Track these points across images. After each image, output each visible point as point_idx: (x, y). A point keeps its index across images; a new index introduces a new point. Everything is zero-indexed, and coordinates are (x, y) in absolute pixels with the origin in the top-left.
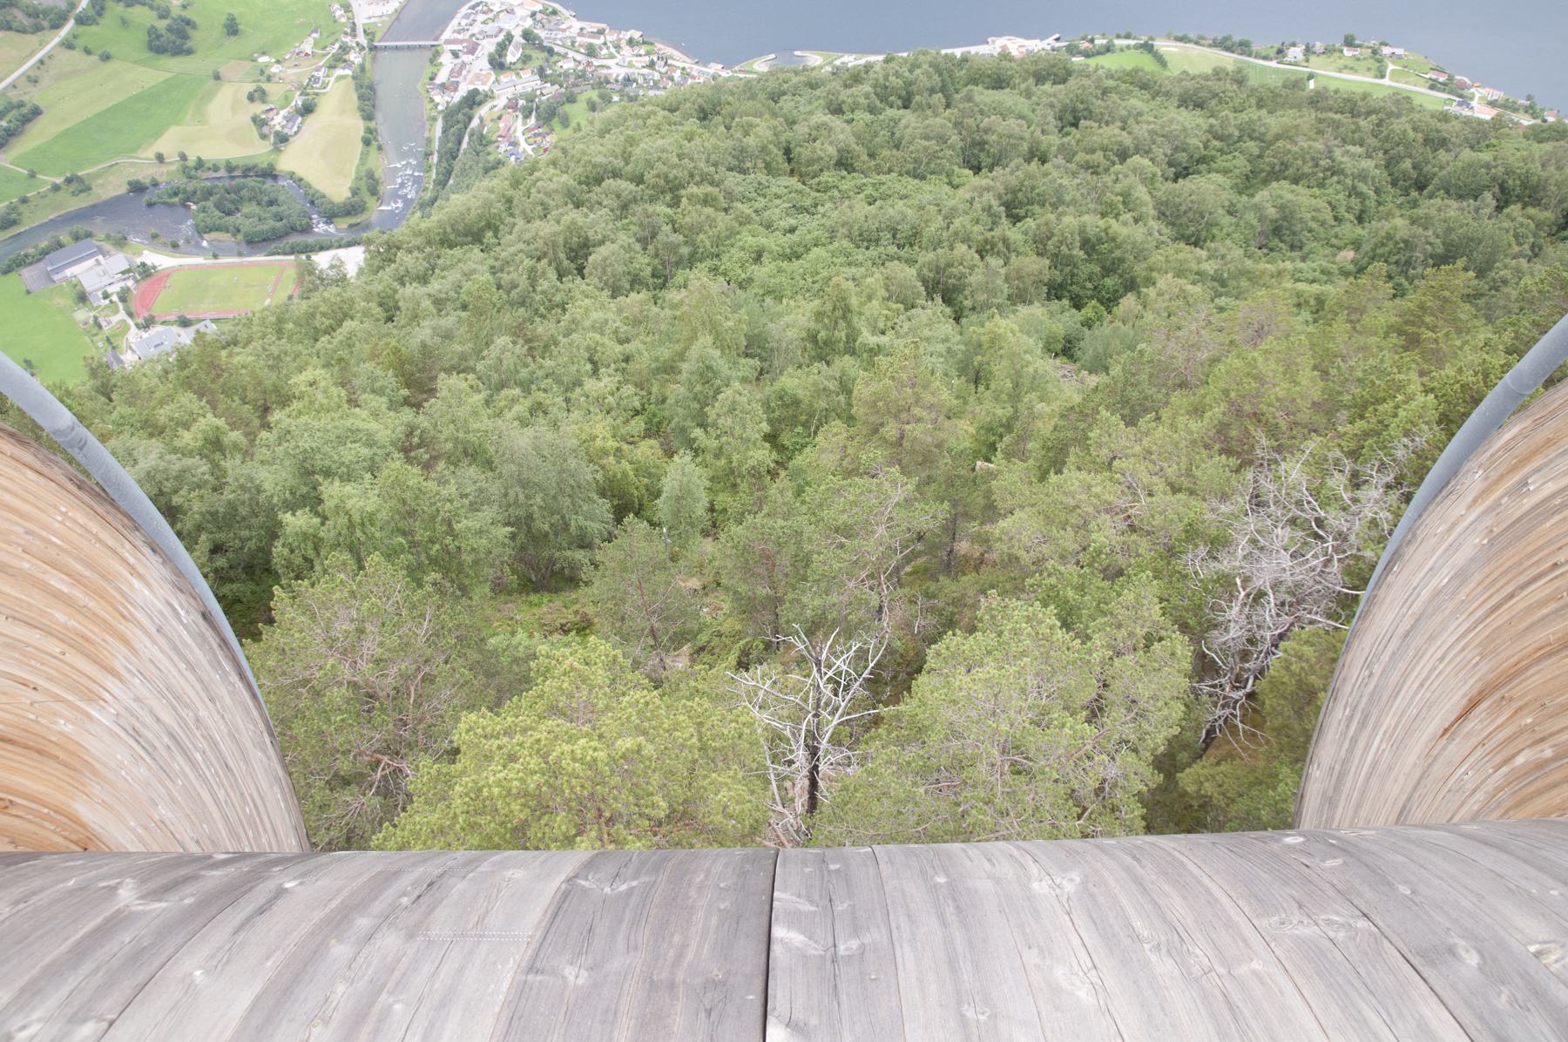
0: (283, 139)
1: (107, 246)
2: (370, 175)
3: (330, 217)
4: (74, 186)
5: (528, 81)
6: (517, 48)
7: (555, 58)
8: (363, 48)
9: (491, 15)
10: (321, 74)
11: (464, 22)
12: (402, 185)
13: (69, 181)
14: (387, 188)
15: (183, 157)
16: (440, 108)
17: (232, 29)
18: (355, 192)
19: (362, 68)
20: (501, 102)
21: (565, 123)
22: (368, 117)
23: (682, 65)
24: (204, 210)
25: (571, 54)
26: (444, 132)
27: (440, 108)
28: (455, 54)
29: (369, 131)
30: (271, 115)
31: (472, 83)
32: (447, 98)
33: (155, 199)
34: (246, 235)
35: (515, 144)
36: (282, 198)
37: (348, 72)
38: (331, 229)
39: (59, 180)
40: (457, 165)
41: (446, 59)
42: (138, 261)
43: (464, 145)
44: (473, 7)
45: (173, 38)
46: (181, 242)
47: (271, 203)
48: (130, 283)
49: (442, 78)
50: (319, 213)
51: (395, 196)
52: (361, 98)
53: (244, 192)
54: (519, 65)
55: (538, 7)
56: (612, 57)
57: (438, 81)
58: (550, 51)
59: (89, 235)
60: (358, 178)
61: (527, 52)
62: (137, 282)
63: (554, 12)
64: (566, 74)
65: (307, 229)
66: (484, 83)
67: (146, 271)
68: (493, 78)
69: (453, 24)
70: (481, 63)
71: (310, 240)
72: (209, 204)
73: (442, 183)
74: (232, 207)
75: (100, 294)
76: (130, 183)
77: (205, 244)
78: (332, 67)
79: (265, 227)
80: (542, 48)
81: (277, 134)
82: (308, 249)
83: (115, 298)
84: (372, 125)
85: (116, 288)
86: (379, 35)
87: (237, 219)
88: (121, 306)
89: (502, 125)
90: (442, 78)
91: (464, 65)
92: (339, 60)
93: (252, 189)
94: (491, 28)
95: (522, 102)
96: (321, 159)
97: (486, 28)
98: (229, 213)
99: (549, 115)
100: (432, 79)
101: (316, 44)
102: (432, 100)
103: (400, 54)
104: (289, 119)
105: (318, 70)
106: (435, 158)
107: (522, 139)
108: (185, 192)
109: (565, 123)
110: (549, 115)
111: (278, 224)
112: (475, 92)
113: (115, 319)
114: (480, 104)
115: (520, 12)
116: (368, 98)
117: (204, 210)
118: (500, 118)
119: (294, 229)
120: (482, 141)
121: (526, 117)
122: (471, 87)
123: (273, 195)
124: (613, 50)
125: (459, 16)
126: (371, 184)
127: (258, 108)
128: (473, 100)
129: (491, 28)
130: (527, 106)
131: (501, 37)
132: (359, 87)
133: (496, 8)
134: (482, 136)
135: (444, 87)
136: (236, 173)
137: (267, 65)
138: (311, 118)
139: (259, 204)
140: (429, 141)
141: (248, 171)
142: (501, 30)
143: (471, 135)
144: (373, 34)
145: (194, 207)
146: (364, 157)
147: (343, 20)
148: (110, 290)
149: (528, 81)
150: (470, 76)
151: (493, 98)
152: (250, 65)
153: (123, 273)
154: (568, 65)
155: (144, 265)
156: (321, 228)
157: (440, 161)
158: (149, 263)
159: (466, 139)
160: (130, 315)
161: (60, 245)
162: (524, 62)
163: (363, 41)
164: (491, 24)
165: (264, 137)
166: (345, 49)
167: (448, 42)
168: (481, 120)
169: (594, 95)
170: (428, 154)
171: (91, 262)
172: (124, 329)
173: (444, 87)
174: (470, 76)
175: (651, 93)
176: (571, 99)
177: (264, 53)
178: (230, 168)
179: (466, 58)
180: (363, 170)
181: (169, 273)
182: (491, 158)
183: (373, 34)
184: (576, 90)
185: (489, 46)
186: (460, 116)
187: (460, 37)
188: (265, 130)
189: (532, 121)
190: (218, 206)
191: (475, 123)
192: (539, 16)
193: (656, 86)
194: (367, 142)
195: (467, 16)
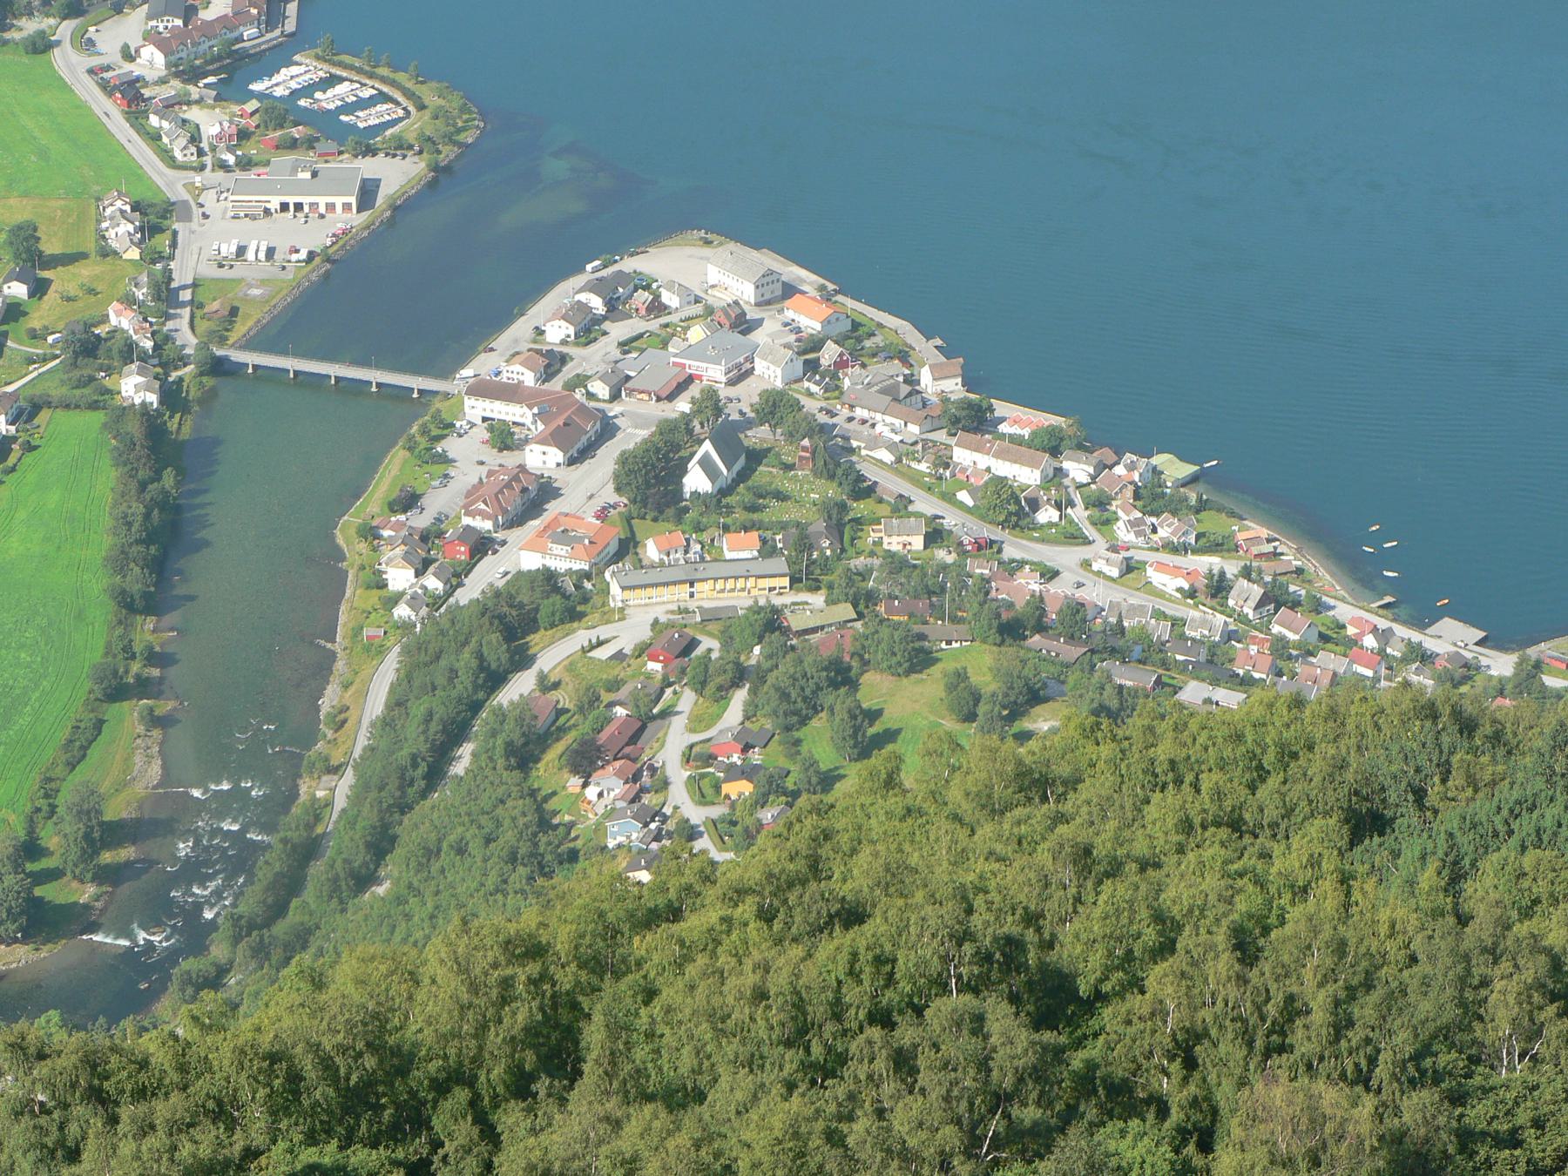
25: (925, 505)
56: (1074, 537)
69: (520, 329)
95: (709, 644)
107: (678, 775)
122: (531, 561)
124: (1079, 513)
175: (1193, 692)
193: (1215, 663)
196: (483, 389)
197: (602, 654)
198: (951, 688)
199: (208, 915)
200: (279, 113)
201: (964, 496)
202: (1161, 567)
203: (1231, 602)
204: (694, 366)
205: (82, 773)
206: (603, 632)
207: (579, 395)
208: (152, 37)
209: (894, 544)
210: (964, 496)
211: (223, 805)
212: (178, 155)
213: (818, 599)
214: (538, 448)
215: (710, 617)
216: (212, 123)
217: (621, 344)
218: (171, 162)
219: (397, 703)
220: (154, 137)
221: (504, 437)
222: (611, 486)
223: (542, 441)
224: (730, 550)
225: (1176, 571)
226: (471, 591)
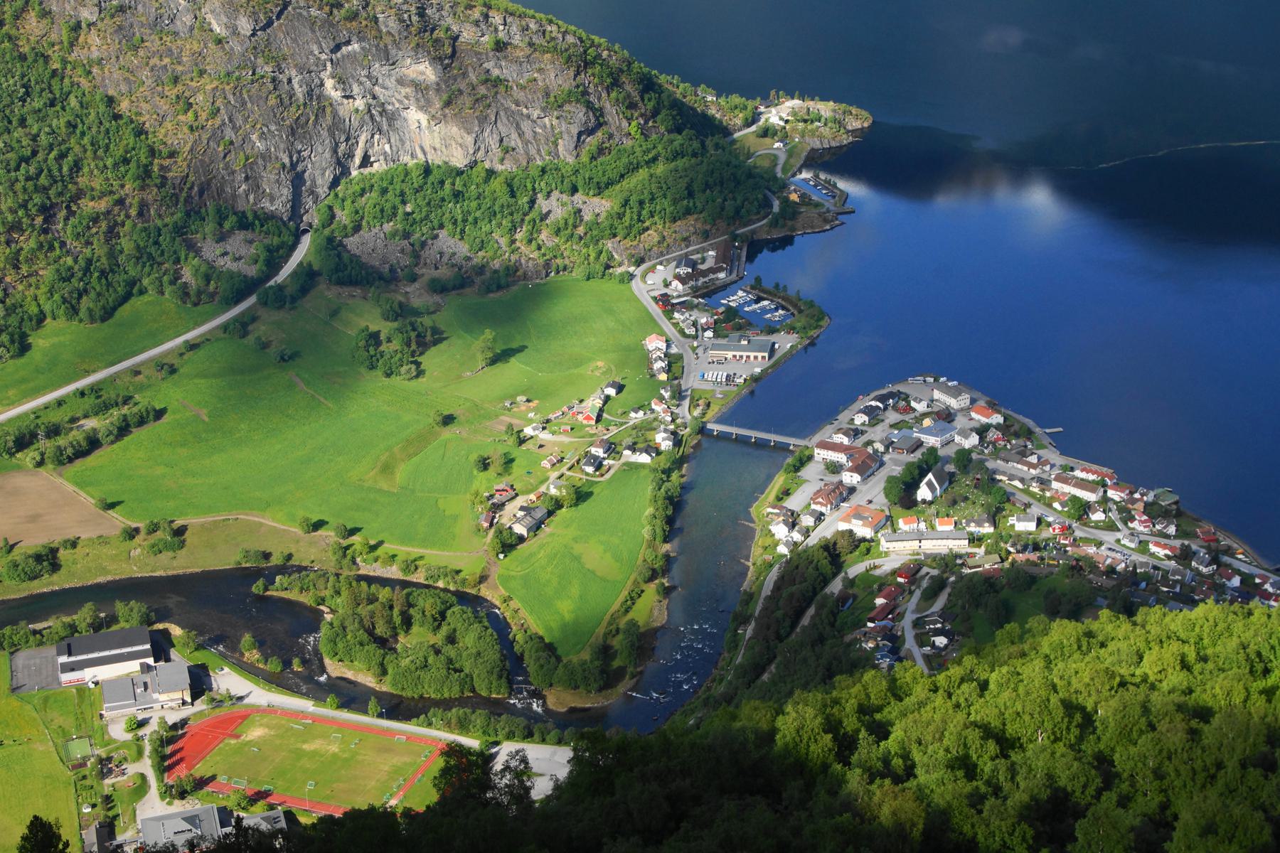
23: (1245, 569)
26: (772, 591)
43: (805, 621)
56: (1110, 527)
69: (843, 417)
115: (960, 422)
122: (843, 526)
124: (1114, 515)
133: (920, 407)
143: (820, 607)
159: (811, 611)
172: (141, 787)
192: (992, 435)
200: (731, 313)
202: (1157, 544)
203: (1193, 563)
205: (630, 616)
207: (870, 450)
208: (678, 277)
210: (1056, 505)
212: (687, 331)
214: (848, 474)
217: (891, 426)
221: (834, 468)
223: (851, 470)
224: (941, 524)
225: (1164, 547)
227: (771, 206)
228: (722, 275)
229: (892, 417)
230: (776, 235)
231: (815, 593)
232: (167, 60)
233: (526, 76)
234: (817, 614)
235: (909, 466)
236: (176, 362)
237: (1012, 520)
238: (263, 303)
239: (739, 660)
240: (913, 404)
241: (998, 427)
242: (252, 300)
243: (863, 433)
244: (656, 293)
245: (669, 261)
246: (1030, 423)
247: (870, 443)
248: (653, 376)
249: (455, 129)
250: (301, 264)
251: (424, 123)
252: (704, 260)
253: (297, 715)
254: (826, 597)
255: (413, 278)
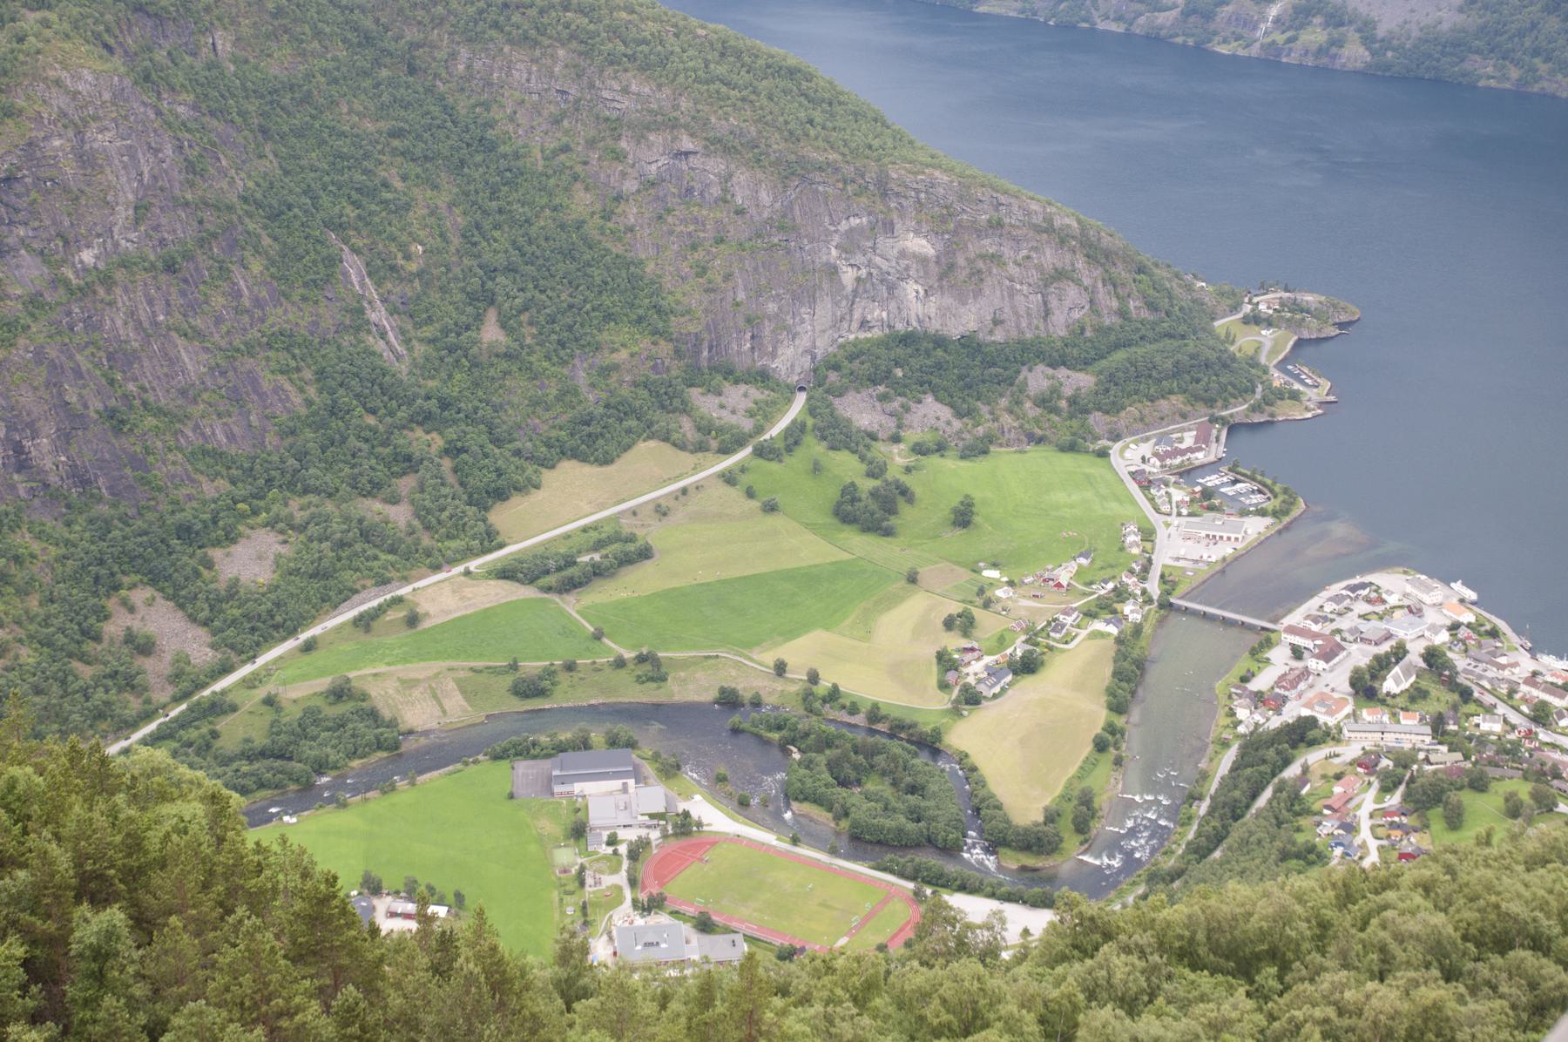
0: (972, 698)
1: (649, 769)
2: (1086, 800)
3: (994, 844)
4: (646, 668)
5: (1409, 732)
6: (1407, 674)
7: (1471, 708)
8: (1149, 601)
9: (1379, 609)
10: (1069, 620)
11: (1329, 608)
12: (1133, 833)
13: (641, 659)
14: (1106, 827)
15: (814, 678)
16: (1241, 729)
17: (963, 517)
18: (1051, 817)
19: (1137, 630)
20: (1351, 751)
21: (1455, 820)
22: (1118, 708)
24: (809, 765)
25: (1502, 709)
26: (1233, 770)
27: (1241, 729)
28: (1297, 653)
29: (1111, 729)
30: (968, 657)
31: (1309, 705)
32: (1258, 717)
33: (746, 726)
34: (855, 825)
35: (1351, 828)
36: (933, 787)
37: (1113, 630)
38: (990, 862)
39: (629, 655)
40: (1237, 831)
41: (1279, 657)
42: (682, 806)
43: (1262, 801)
44: (1353, 588)
45: (873, 506)
46: (755, 802)
47: (912, 789)
48: (655, 835)
49: (1262, 683)
50: (981, 831)
51: (1113, 846)
52: (1118, 674)
53: (880, 760)
54: (1401, 701)
55: (1468, 617)
57: (1254, 685)
58: (1466, 695)
59: (631, 745)
60: (1066, 797)
61: (1424, 684)
62: (665, 836)
63: (1494, 633)
64: (1482, 741)
65: (951, 850)
66: (1330, 713)
67: (685, 826)
68: (1348, 709)
69: (1312, 605)
70: (1337, 677)
71: (951, 868)
72: (821, 759)
73: (1200, 851)
74: (853, 775)
75: (605, 835)
76: (723, 690)
77: (788, 815)
78: (1090, 615)
79: (888, 823)
80: (1452, 684)
81: (966, 688)
82: (941, 881)
83: (623, 849)
84: (1120, 721)
85: (630, 835)
86: (1182, 589)
87: (853, 796)
88: (625, 864)
89: (1338, 789)
90: (1262, 683)
91: (1306, 672)
92: (1106, 607)
93: (894, 758)
94: (1373, 628)
96: (1018, 749)
97: (1364, 626)
98: (844, 783)
99: (1428, 798)
100: (1244, 680)
101: (1079, 573)
102: (1232, 714)
103: (1207, 626)
104: (993, 672)
105: (1067, 613)
106: (1203, 808)
107: (1365, 825)
108: (794, 729)
109: (1455, 820)
110: (1428, 798)
111: (911, 826)
112: (1312, 722)
113: (608, 880)
114: (1312, 743)
115: (1431, 616)
116: (1129, 675)
117: (809, 765)
118: (1338, 777)
119: (930, 842)
120: (1294, 805)
121: (1386, 789)
122: (1306, 712)
123: (921, 779)
125: (1325, 594)
126: (1081, 813)
127: (954, 642)
128: (1303, 734)
129: (1373, 628)
130: (1394, 772)
131: (1385, 647)
132: (1121, 656)
133: (1392, 600)
134: (1295, 797)
135: (1259, 699)
136: (880, 727)
137: (993, 584)
138: (1028, 681)
139: (894, 784)
140: (1205, 776)
141: (899, 729)
142: (1389, 637)
143: (1279, 790)
144: (1174, 584)
145: (797, 756)
146: (1087, 767)
147: (1135, 551)
148: (623, 834)
149: (1409, 732)
150: (1310, 694)
151: (1337, 740)
152: (966, 574)
153: (652, 816)
154: (1490, 726)
155: (686, 814)
156: (975, 855)
157: (1211, 812)
158: (695, 815)
159: (1268, 793)
160: (633, 882)
161: (585, 745)
162: (1413, 699)
163: (1154, 588)
164: (1375, 623)
165: (944, 686)
166: (1121, 594)
167: (1292, 630)
168: (1306, 769)
169: (1524, 790)
170: (1194, 797)
171: (616, 784)
172: (614, 899)
173: (1259, 699)
174: (1310, 694)
176: (1479, 784)
177: (995, 565)
178: (875, 715)
179: (1314, 664)
180: (1079, 786)
181: (716, 840)
182: (1300, 838)
183: (1174, 584)
184: (1492, 772)
185: (1359, 656)
186: (1271, 754)
187: (1315, 628)
188: (951, 677)
189: (1394, 799)
190: (832, 766)
191: (1292, 772)
192: (1463, 633)
194: (1101, 746)
195: (1337, 599)
196: (1292, 630)
197: (1336, 761)
198: (1507, 800)
199: (1137, 855)
200: (1207, 494)
201: (1524, 708)
204: (1393, 630)
206: (1338, 750)
208: (1156, 455)
209: (1485, 727)
211: (1148, 806)
213: (1444, 748)
215: (1389, 752)
216: (1178, 495)
218: (1157, 510)
219: (1235, 768)
220: (1152, 500)
222: (1347, 683)
223: (1318, 657)
226: (1275, 722)
227: (1254, 392)
228: (1200, 455)
229: (1362, 607)
230: (1258, 418)
231: (1274, 775)
232: (692, 228)
233: (1024, 253)
234: (1274, 797)
235: (1377, 658)
236: (672, 503)
237: (1476, 720)
238: (760, 452)
239: (1191, 836)
240: (1384, 596)
241: (1469, 626)
242: (749, 450)
243: (1332, 620)
244: (1133, 469)
245: (1147, 439)
246: (1502, 625)
247: (1339, 631)
248: (1122, 549)
249: (951, 300)
250: (794, 422)
251: (922, 293)
252: (1181, 440)
253: (761, 846)
254: (1283, 782)
255: (896, 439)
